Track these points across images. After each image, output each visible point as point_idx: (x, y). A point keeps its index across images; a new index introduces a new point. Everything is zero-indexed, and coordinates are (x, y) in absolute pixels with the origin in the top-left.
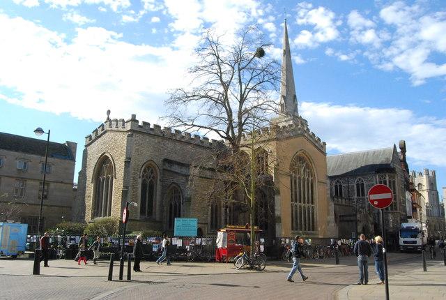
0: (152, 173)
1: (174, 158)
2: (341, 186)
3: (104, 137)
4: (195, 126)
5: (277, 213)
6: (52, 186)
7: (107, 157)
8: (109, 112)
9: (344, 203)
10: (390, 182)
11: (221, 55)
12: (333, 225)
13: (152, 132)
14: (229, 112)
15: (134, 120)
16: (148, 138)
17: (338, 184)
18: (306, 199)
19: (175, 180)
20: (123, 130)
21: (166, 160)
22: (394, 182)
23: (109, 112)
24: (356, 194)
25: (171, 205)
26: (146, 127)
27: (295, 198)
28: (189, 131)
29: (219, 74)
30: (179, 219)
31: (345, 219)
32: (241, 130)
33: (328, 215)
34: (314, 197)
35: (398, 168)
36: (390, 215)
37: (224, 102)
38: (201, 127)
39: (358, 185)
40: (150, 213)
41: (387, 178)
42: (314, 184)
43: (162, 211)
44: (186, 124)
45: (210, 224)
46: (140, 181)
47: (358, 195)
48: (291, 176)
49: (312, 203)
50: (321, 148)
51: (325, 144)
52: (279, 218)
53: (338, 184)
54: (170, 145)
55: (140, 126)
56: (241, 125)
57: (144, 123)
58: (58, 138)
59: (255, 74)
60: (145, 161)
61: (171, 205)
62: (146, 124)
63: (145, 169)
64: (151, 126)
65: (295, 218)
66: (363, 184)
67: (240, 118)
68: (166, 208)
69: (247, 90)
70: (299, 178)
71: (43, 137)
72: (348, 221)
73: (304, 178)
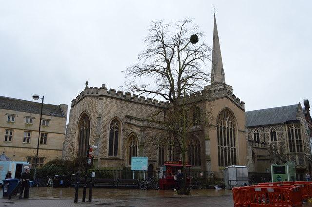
0: (117, 124)
1: (133, 114)
2: (258, 134)
3: (84, 100)
4: (146, 91)
5: (207, 153)
6: (50, 135)
7: (85, 114)
8: (87, 83)
9: (260, 146)
10: (296, 130)
11: (166, 41)
12: (251, 162)
13: (117, 97)
14: (171, 81)
15: (104, 88)
16: (114, 101)
17: (256, 132)
18: (230, 144)
20: (97, 95)
21: (127, 116)
22: (299, 130)
23: (87, 83)
24: (270, 140)
25: (130, 147)
26: (113, 93)
27: (221, 141)
28: (143, 95)
29: (164, 54)
30: (134, 158)
31: (261, 158)
32: (179, 94)
34: (236, 142)
36: (297, 155)
37: (167, 73)
38: (151, 92)
39: (271, 133)
40: (116, 154)
41: (294, 128)
42: (236, 132)
43: (124, 152)
44: (140, 91)
45: (158, 162)
46: (108, 131)
47: (272, 140)
50: (240, 105)
51: (243, 103)
52: (209, 157)
53: (256, 132)
54: (130, 105)
55: (108, 93)
56: (179, 91)
57: (111, 90)
58: (57, 103)
59: (189, 54)
60: (112, 116)
61: (130, 147)
62: (112, 91)
63: (112, 122)
64: (116, 92)
65: (221, 158)
66: (275, 132)
67: (179, 84)
68: (127, 150)
69: (184, 65)
71: (40, 101)
72: (264, 160)
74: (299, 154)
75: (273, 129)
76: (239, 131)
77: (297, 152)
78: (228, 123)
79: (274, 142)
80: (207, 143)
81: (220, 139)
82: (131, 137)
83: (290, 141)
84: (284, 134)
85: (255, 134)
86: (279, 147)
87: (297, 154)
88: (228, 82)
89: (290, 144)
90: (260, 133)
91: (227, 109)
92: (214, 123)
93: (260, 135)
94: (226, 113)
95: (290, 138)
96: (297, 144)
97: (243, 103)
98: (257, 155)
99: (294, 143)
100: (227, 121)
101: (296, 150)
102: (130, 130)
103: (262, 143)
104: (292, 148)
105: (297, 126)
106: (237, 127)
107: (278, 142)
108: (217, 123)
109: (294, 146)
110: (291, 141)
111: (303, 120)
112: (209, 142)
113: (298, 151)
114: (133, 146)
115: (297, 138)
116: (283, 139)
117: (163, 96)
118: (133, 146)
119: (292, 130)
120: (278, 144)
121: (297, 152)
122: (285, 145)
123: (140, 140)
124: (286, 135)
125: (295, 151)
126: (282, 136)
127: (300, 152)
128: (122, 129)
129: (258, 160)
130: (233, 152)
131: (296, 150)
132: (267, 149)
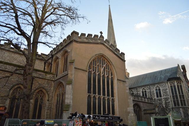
2: (145, 92)
10: (178, 86)
12: (133, 115)
17: (144, 91)
22: (181, 86)
31: (148, 112)
33: (128, 106)
35: (183, 78)
36: (181, 109)
41: (176, 84)
47: (157, 96)
48: (90, 73)
49: (113, 96)
50: (121, 57)
53: (144, 91)
66: (159, 89)
70: (99, 75)
73: (104, 76)
74: (183, 108)
75: (157, 86)
76: (118, 80)
77: (180, 106)
78: (104, 70)
79: (159, 98)
80: (69, 88)
81: (92, 86)
83: (173, 96)
84: (167, 91)
85: (143, 92)
86: (164, 102)
87: (181, 107)
88: (118, 47)
89: (174, 98)
90: (147, 91)
91: (102, 56)
92: (85, 66)
93: (147, 93)
94: (101, 58)
95: (173, 94)
96: (180, 98)
97: (123, 54)
98: (143, 109)
99: (177, 98)
100: (102, 70)
101: (180, 104)
103: (149, 98)
104: (176, 103)
105: (178, 82)
106: (116, 75)
107: (162, 97)
108: (90, 68)
109: (178, 101)
110: (174, 96)
111: (183, 78)
112: (70, 86)
113: (182, 105)
115: (179, 93)
116: (167, 95)
117: (6, 24)
119: (175, 86)
120: (163, 100)
121: (180, 106)
122: (169, 100)
124: (169, 91)
125: (178, 105)
126: (166, 93)
127: (184, 106)
129: (145, 114)
130: (111, 103)
131: (180, 104)
132: (153, 104)
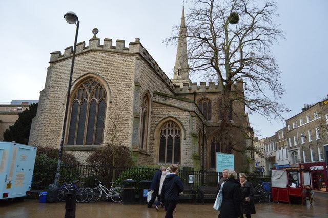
8: (95, 31)
15: (137, 42)
19: (171, 114)
20: (125, 51)
21: (156, 93)
23: (95, 31)
82: (167, 122)
102: (163, 113)
114: (170, 138)
118: (170, 138)
123: (188, 129)
128: (150, 110)
